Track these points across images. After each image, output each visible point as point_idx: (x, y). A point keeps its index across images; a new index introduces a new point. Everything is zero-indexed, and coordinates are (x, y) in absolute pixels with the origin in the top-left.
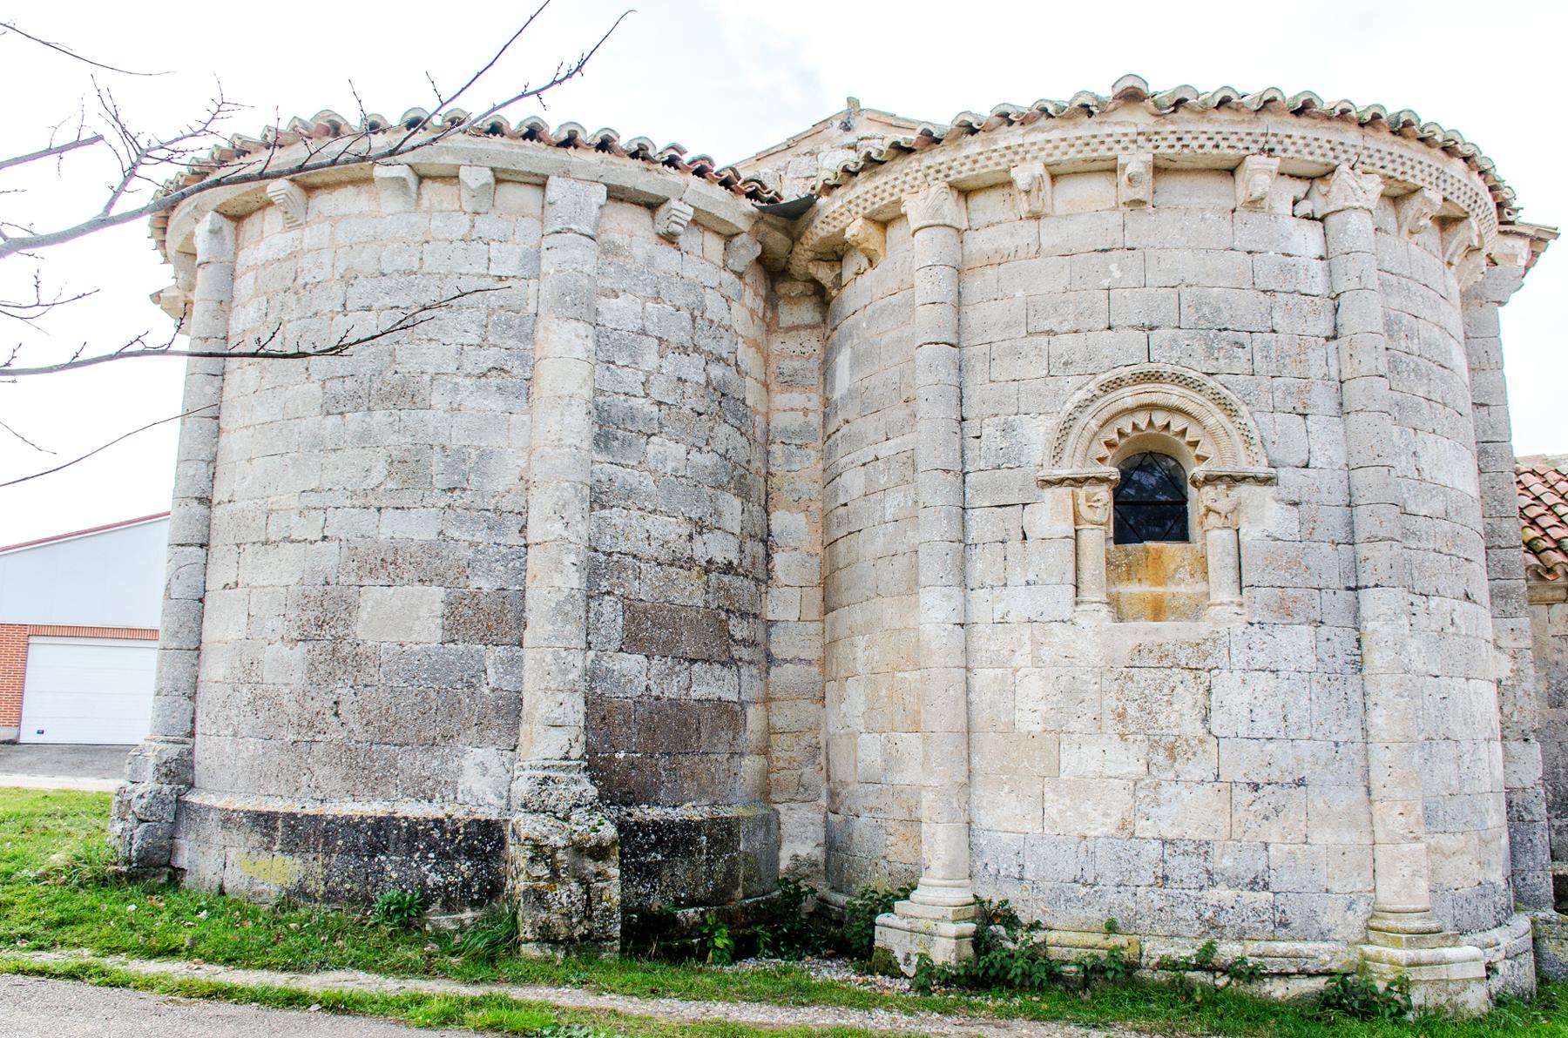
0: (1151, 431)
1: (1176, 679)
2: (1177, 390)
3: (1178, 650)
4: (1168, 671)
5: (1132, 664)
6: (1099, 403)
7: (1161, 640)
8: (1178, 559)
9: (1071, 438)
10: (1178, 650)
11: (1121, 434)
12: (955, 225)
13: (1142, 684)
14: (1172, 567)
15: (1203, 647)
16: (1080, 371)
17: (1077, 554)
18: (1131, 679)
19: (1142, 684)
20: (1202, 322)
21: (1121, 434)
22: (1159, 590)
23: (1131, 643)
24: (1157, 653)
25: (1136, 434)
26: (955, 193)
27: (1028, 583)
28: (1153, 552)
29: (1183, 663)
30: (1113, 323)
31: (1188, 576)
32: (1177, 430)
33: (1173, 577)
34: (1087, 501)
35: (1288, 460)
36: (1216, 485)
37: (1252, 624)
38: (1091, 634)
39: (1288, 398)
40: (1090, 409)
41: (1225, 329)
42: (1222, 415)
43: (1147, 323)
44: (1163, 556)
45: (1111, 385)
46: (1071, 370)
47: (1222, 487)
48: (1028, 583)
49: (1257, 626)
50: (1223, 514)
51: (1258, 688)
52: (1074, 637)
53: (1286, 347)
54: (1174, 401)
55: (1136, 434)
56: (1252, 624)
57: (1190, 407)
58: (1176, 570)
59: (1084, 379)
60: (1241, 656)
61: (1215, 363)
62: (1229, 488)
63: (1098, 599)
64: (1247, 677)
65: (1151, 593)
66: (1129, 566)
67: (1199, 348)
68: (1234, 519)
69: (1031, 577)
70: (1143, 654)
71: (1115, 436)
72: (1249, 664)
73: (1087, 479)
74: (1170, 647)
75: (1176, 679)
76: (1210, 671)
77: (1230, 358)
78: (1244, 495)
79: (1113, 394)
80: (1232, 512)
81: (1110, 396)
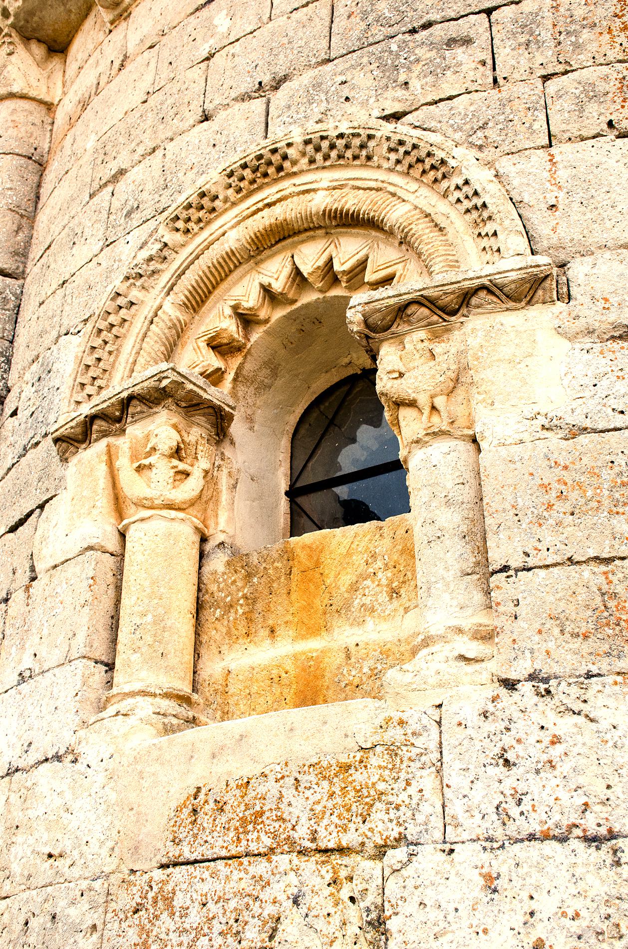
0: (309, 297)
1: (279, 890)
2: (326, 178)
3: (289, 793)
4: (261, 867)
5: (174, 851)
6: (178, 261)
7: (249, 770)
8: (359, 560)
9: (128, 346)
10: (289, 793)
11: (246, 320)
12: (33, 93)
13: (195, 918)
14: (346, 580)
15: (359, 777)
16: (148, 213)
17: (119, 588)
18: (169, 901)
19: (195, 918)
20: (375, 30)
21: (246, 320)
22: (314, 645)
23: (179, 791)
24: (235, 811)
25: (279, 314)
26: (38, 50)
27: (22, 678)
28: (302, 555)
29: (302, 833)
30: (209, 106)
31: (384, 597)
32: (346, 267)
33: (348, 605)
34: (134, 457)
35: (598, 236)
36: (399, 338)
37: (510, 685)
38: (101, 779)
39: (592, 108)
40: (164, 279)
41: (428, 25)
42: (424, 191)
43: (266, 79)
44: (326, 559)
45: (194, 214)
46: (137, 217)
47: (416, 338)
48: (22, 678)
49: (526, 688)
50: (423, 400)
51: (546, 906)
52: (68, 796)
53: (579, 13)
54: (320, 202)
55: (279, 314)
56: (510, 685)
57: (352, 202)
58: (354, 588)
59: (152, 224)
60: (477, 794)
61: (400, 93)
62: (436, 336)
63: (137, 686)
64: (501, 863)
65: (295, 657)
66: (251, 600)
67: (363, 80)
68: (460, 411)
69: (28, 662)
70: (204, 820)
71: (231, 327)
72: (504, 817)
73: (126, 403)
74: (270, 788)
75: (279, 890)
76: (380, 852)
77: (436, 72)
78: (474, 342)
79: (205, 234)
80: (450, 393)
81: (198, 240)
